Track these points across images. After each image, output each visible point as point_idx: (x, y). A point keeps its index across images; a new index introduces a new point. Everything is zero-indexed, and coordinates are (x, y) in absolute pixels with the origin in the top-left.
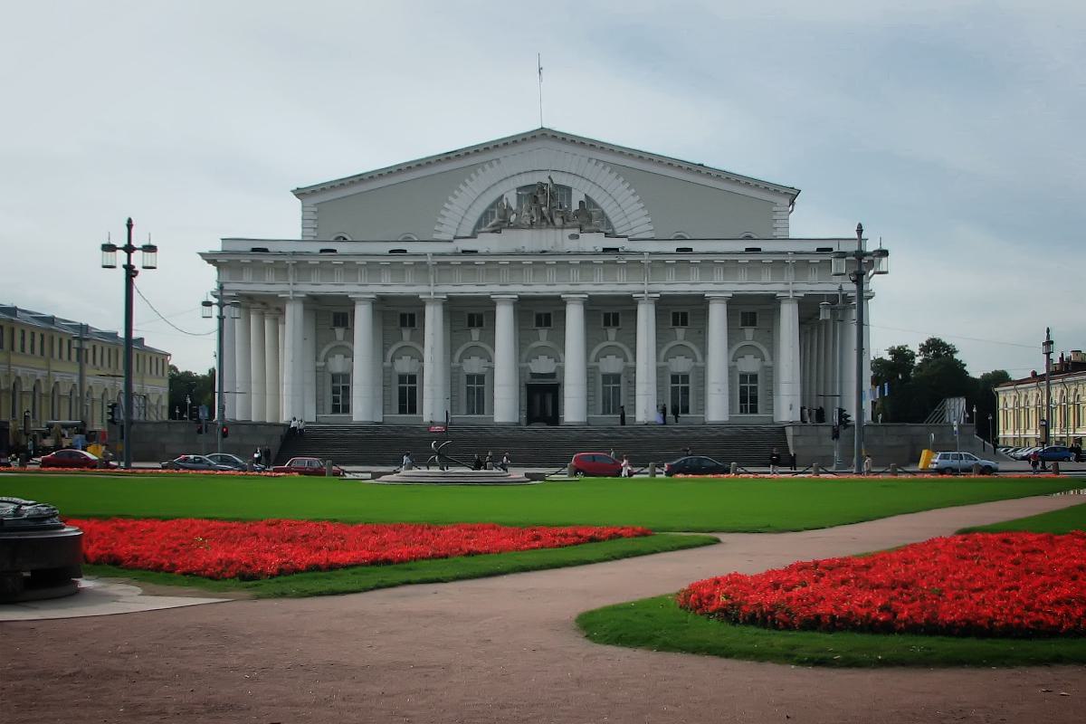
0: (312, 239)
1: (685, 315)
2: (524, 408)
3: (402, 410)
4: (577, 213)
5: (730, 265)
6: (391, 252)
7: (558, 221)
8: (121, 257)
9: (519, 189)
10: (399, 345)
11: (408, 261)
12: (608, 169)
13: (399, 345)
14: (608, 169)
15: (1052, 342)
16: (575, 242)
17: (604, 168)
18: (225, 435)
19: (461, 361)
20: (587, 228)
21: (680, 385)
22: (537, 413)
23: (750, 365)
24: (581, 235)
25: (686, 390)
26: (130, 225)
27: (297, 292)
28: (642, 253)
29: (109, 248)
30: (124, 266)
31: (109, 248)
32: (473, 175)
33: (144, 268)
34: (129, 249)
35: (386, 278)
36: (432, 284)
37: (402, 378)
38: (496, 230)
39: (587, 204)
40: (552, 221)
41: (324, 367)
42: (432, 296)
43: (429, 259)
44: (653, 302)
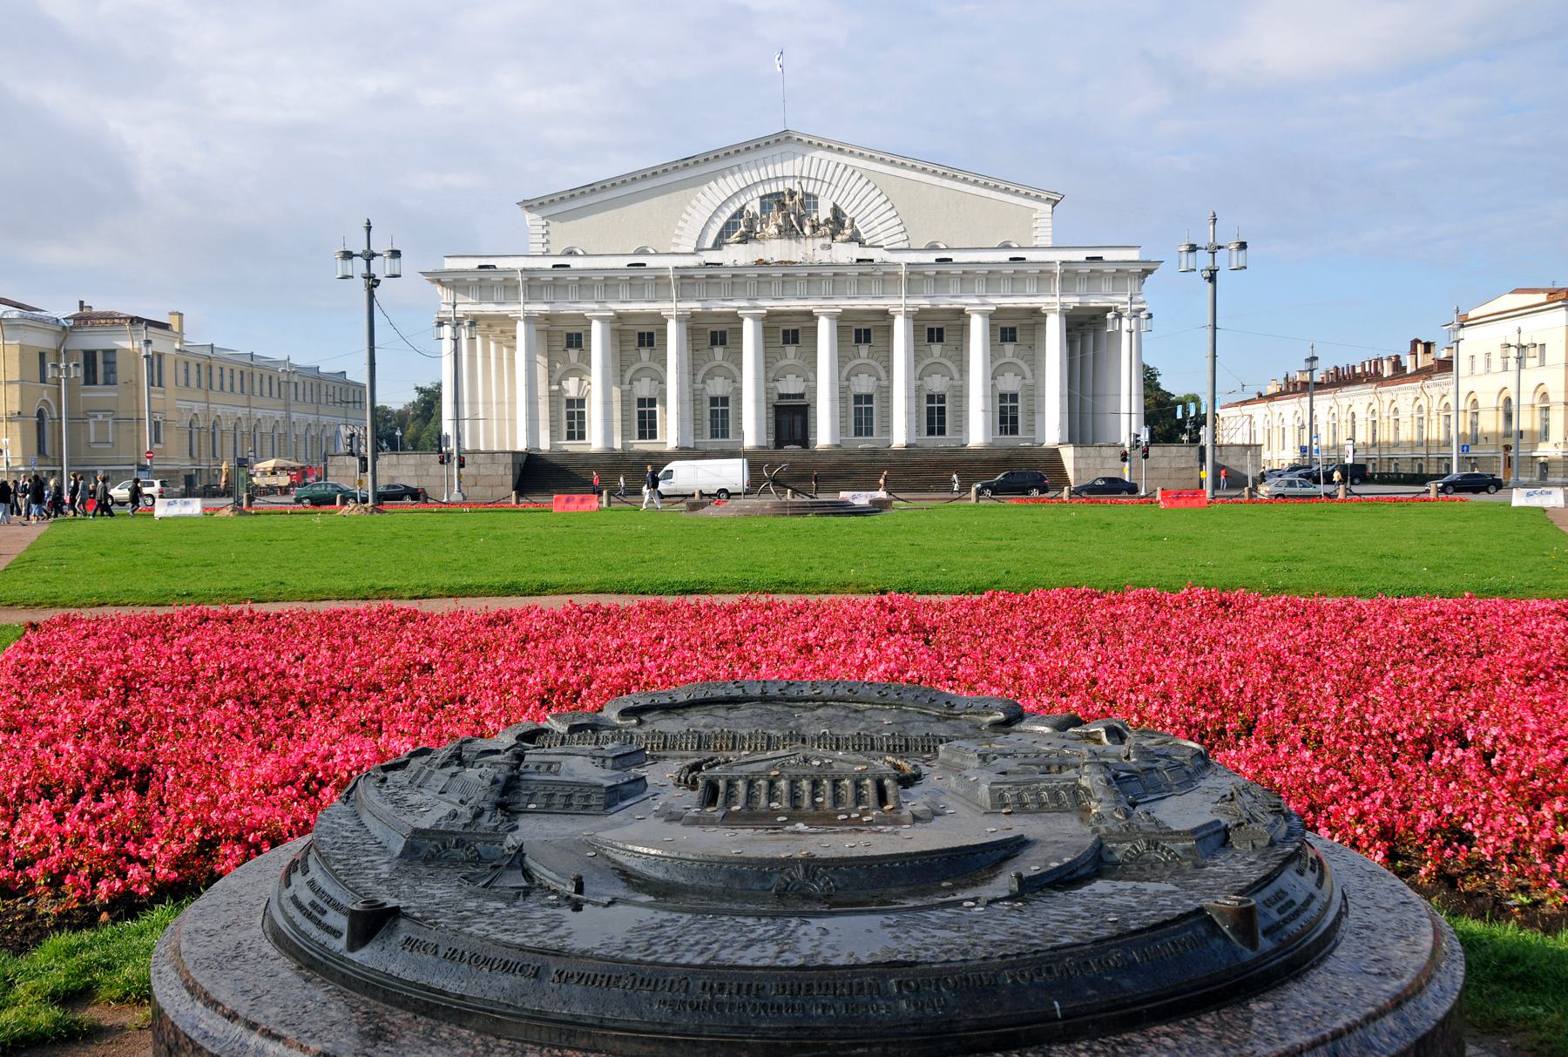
1: (940, 331)
2: (772, 431)
7: (807, 230)
8: (359, 265)
9: (762, 198)
10: (637, 366)
13: (637, 366)
15: (1316, 358)
16: (828, 252)
18: (461, 465)
19: (703, 382)
21: (936, 405)
23: (1009, 384)
25: (942, 410)
26: (369, 229)
29: (348, 255)
31: (348, 255)
34: (370, 256)
38: (745, 239)
39: (837, 215)
41: (559, 390)
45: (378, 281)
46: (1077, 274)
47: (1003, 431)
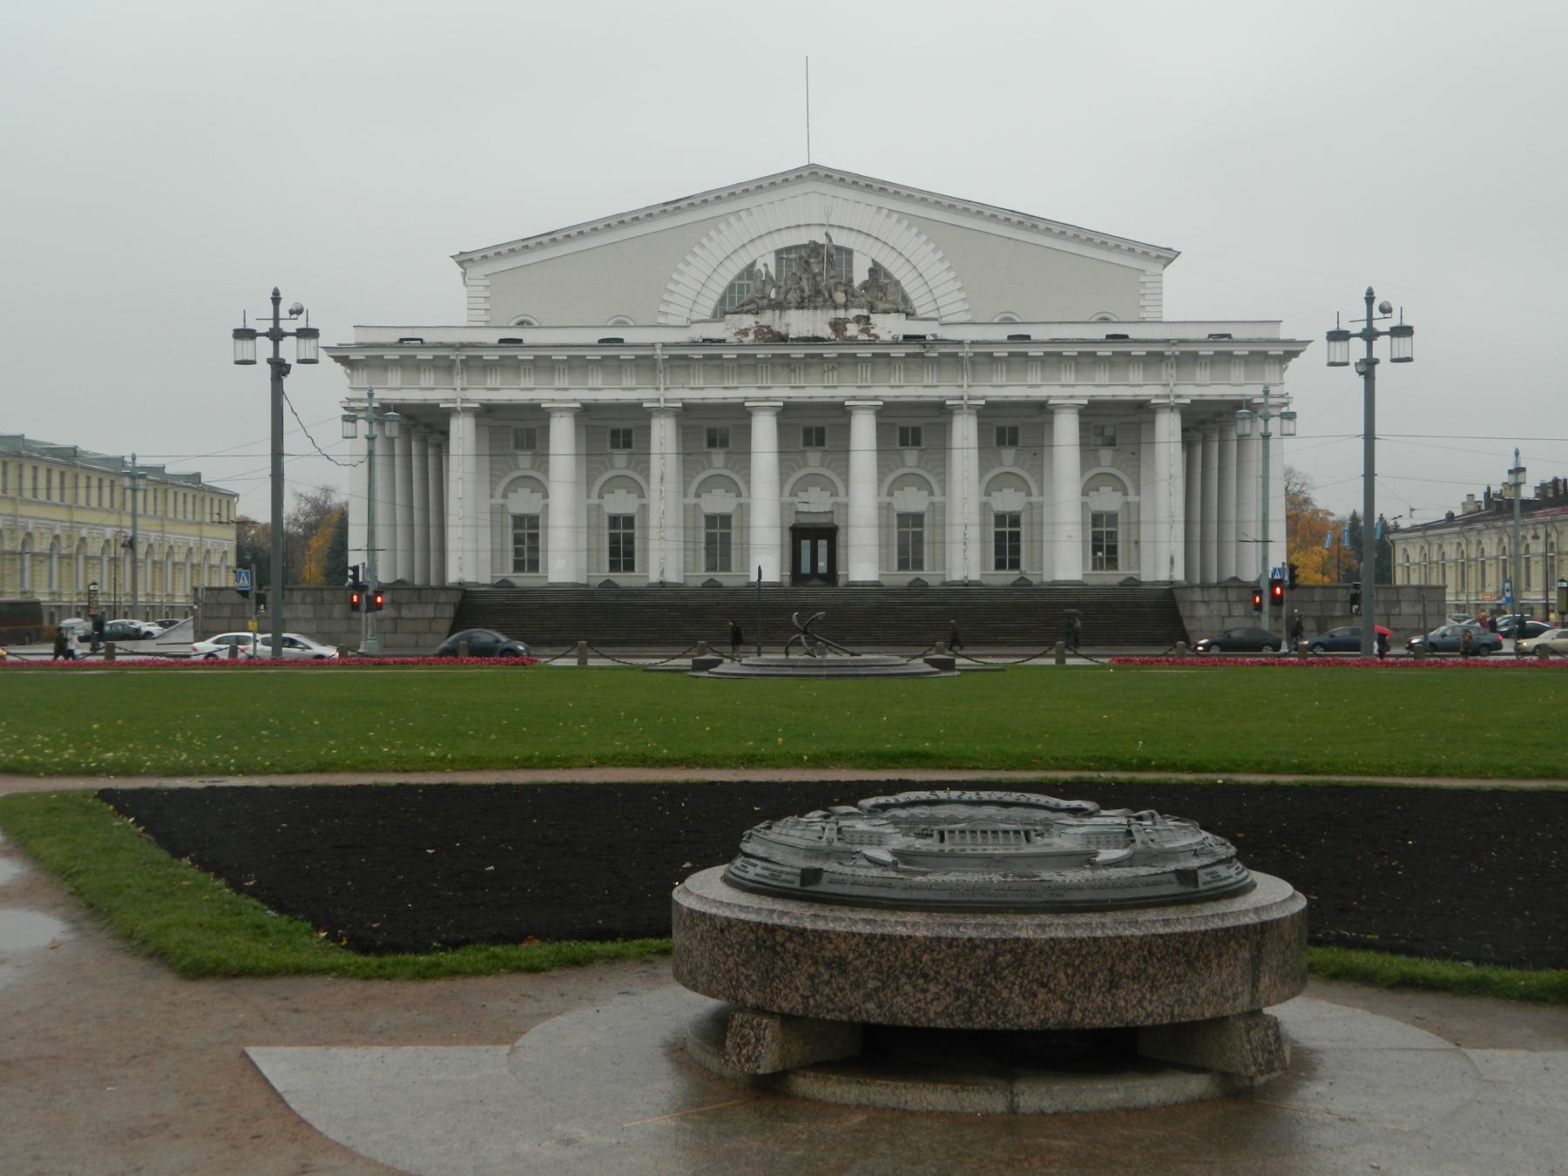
0: (483, 324)
3: (614, 566)
4: (865, 286)
5: (1086, 359)
6: (600, 341)
7: (840, 297)
8: (264, 347)
9: (778, 252)
11: (626, 354)
12: (905, 223)
14: (905, 223)
17: (899, 221)
20: (881, 306)
21: (1007, 529)
22: (806, 568)
24: (871, 315)
25: (1015, 537)
27: (467, 400)
28: (961, 343)
29: (244, 334)
30: (269, 361)
31: (244, 334)
32: (713, 233)
33: (299, 361)
34: (276, 335)
35: (596, 380)
36: (662, 387)
37: (614, 521)
40: (831, 296)
42: (662, 405)
43: (658, 352)
44: (974, 411)
45: (290, 366)
46: (1195, 355)
47: (1097, 564)
